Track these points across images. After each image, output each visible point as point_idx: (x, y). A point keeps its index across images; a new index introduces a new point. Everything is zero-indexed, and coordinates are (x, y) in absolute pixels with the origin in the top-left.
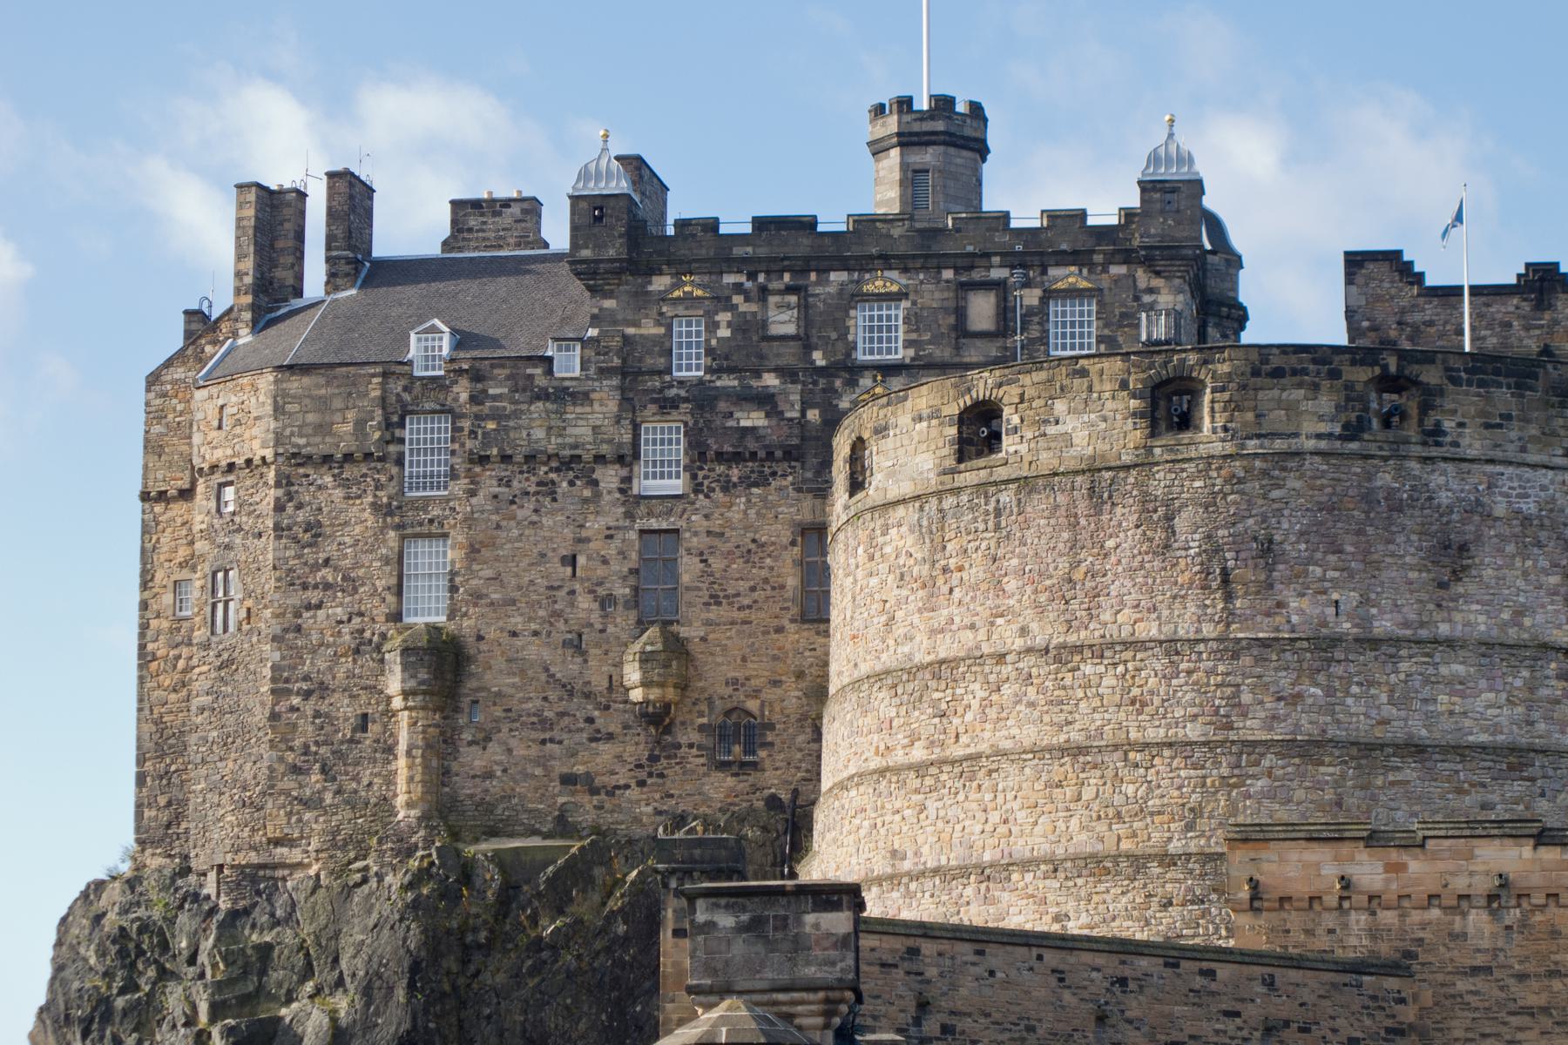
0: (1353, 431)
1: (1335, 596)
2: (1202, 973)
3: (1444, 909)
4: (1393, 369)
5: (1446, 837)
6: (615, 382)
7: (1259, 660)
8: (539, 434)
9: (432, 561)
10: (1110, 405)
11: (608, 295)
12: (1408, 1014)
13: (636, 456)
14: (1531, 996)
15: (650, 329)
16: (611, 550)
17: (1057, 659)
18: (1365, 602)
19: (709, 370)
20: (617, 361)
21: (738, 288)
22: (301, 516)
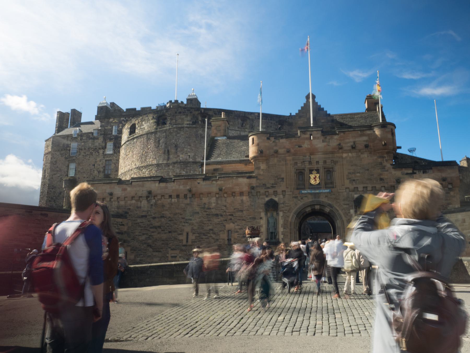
0: (194, 123)
1: (189, 154)
2: (42, 214)
3: (136, 200)
4: (203, 112)
5: (137, 181)
6: (103, 136)
7: (174, 167)
8: (90, 145)
9: (72, 166)
10: (151, 121)
11: (103, 122)
12: (125, 229)
13: (106, 148)
14: (156, 223)
15: (109, 127)
16: (101, 163)
17: (139, 169)
18: (195, 155)
19: (118, 133)
20: (103, 133)
21: (123, 120)
22: (55, 160)
